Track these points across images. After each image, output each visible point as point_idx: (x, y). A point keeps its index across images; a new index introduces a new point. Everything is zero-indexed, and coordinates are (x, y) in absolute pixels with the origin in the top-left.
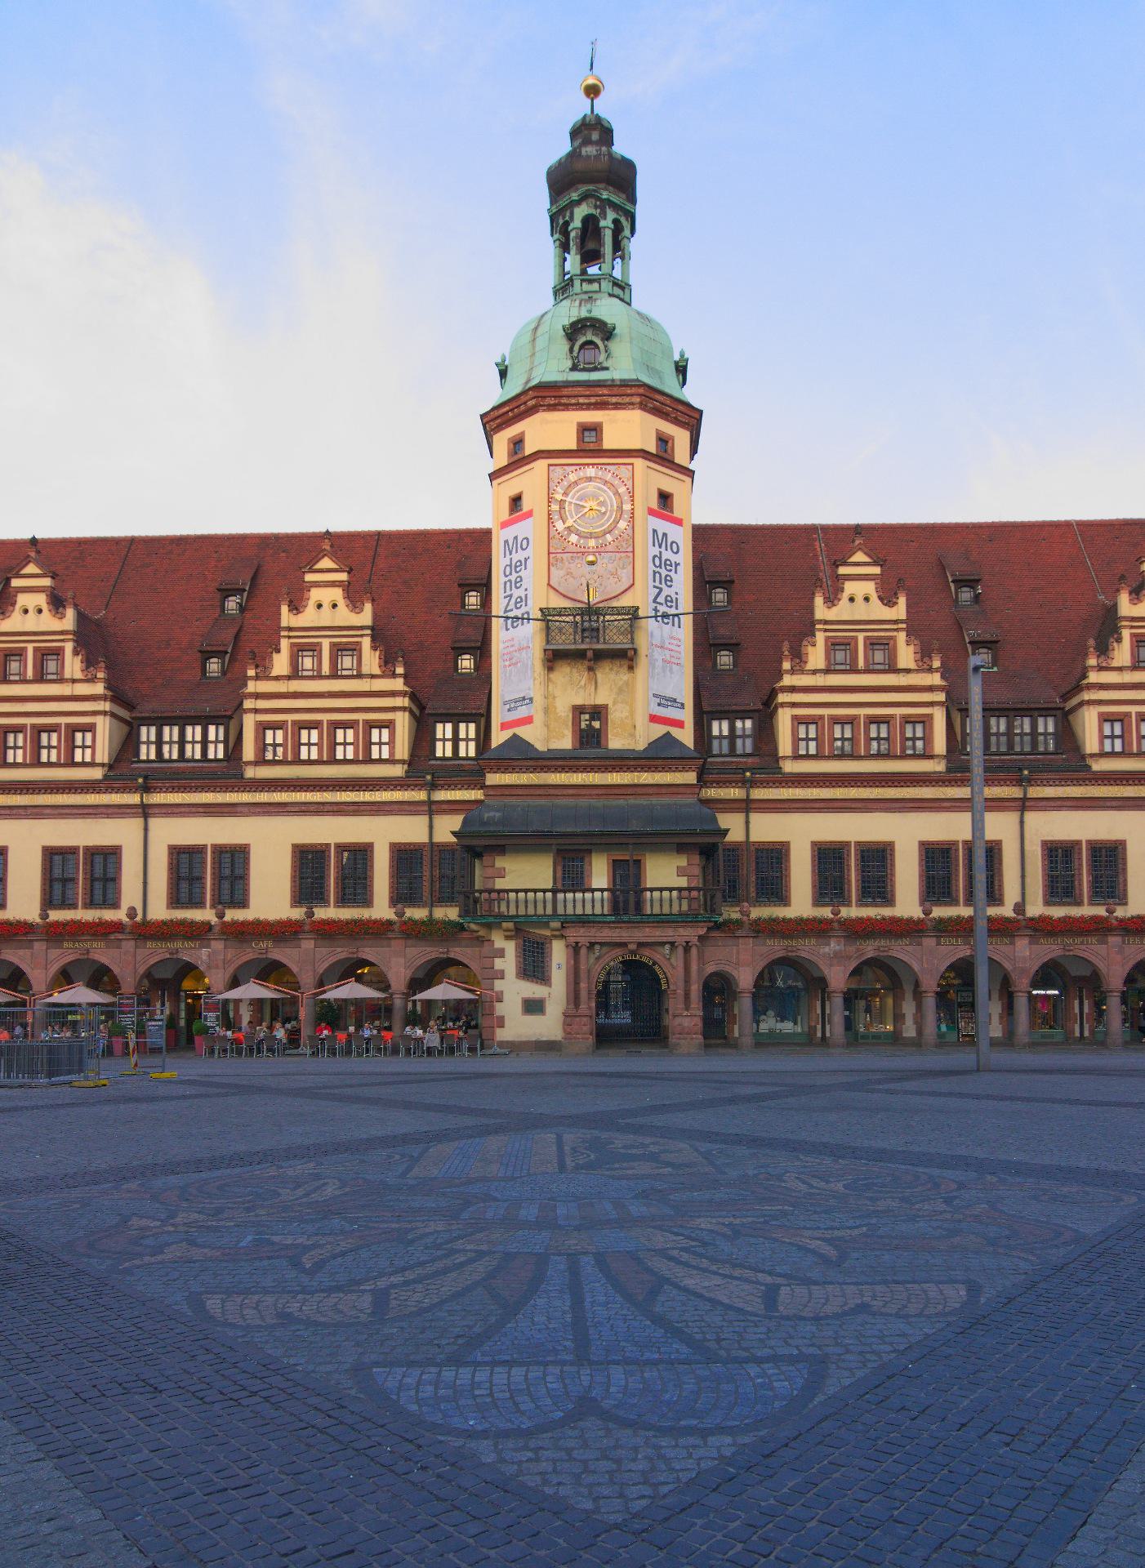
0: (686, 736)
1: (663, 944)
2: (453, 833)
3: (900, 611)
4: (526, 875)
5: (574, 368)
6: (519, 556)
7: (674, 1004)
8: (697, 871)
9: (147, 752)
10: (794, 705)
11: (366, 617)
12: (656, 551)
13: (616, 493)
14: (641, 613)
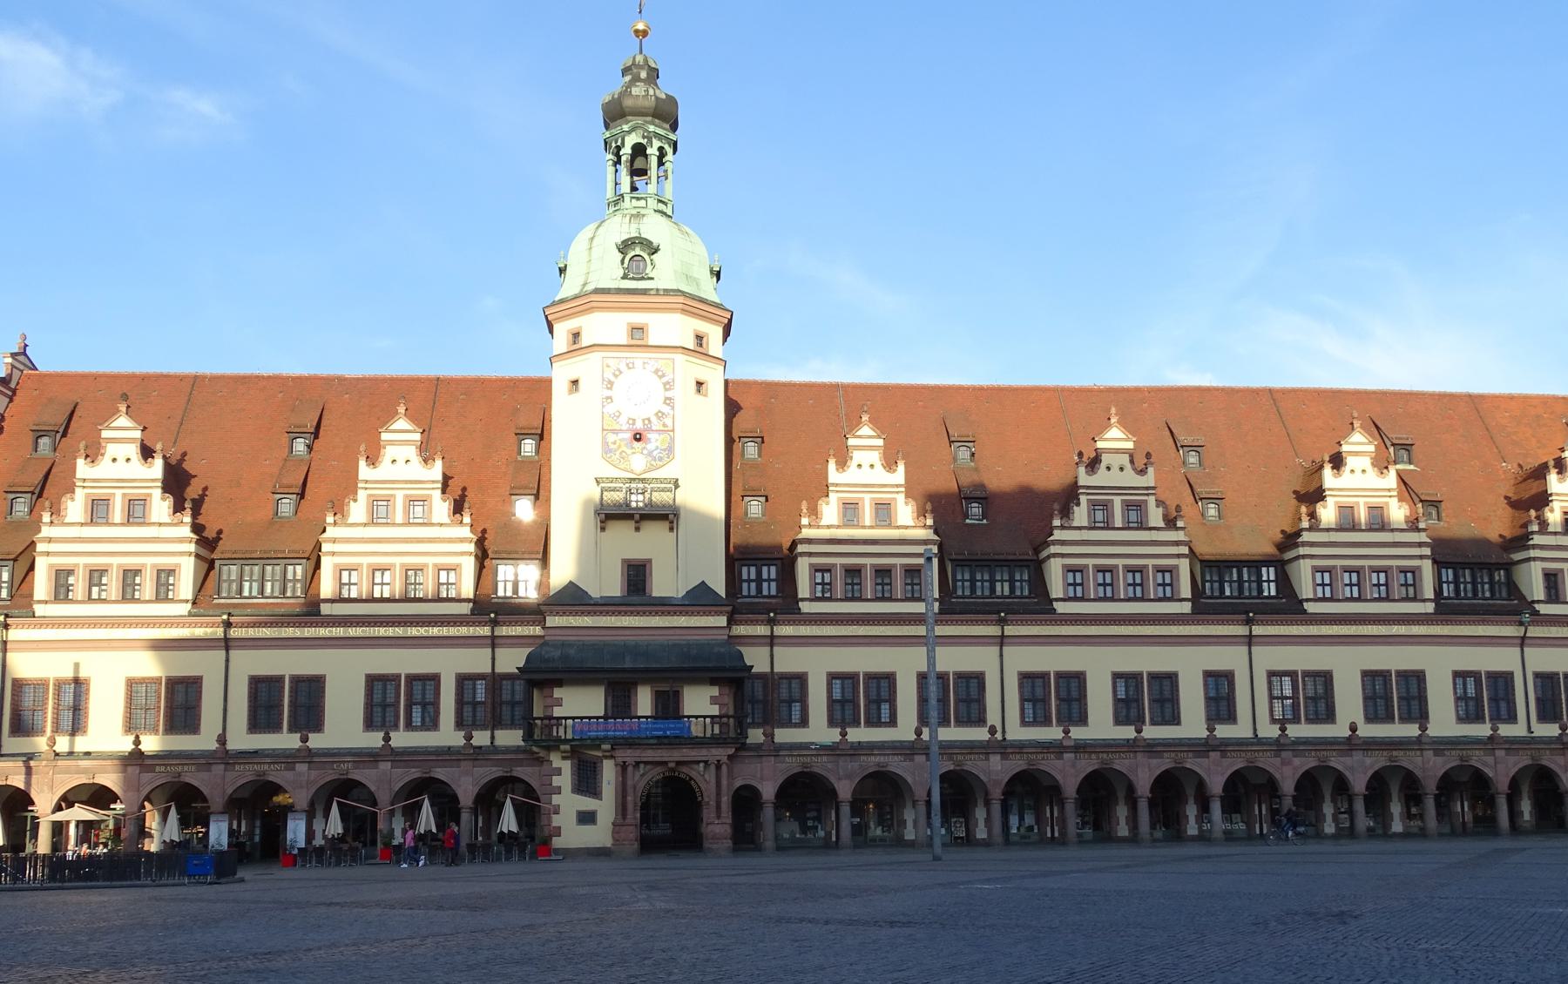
0: (720, 587)
1: (698, 762)
3: (899, 476)
4: (581, 704)
7: (708, 814)
10: (810, 554)
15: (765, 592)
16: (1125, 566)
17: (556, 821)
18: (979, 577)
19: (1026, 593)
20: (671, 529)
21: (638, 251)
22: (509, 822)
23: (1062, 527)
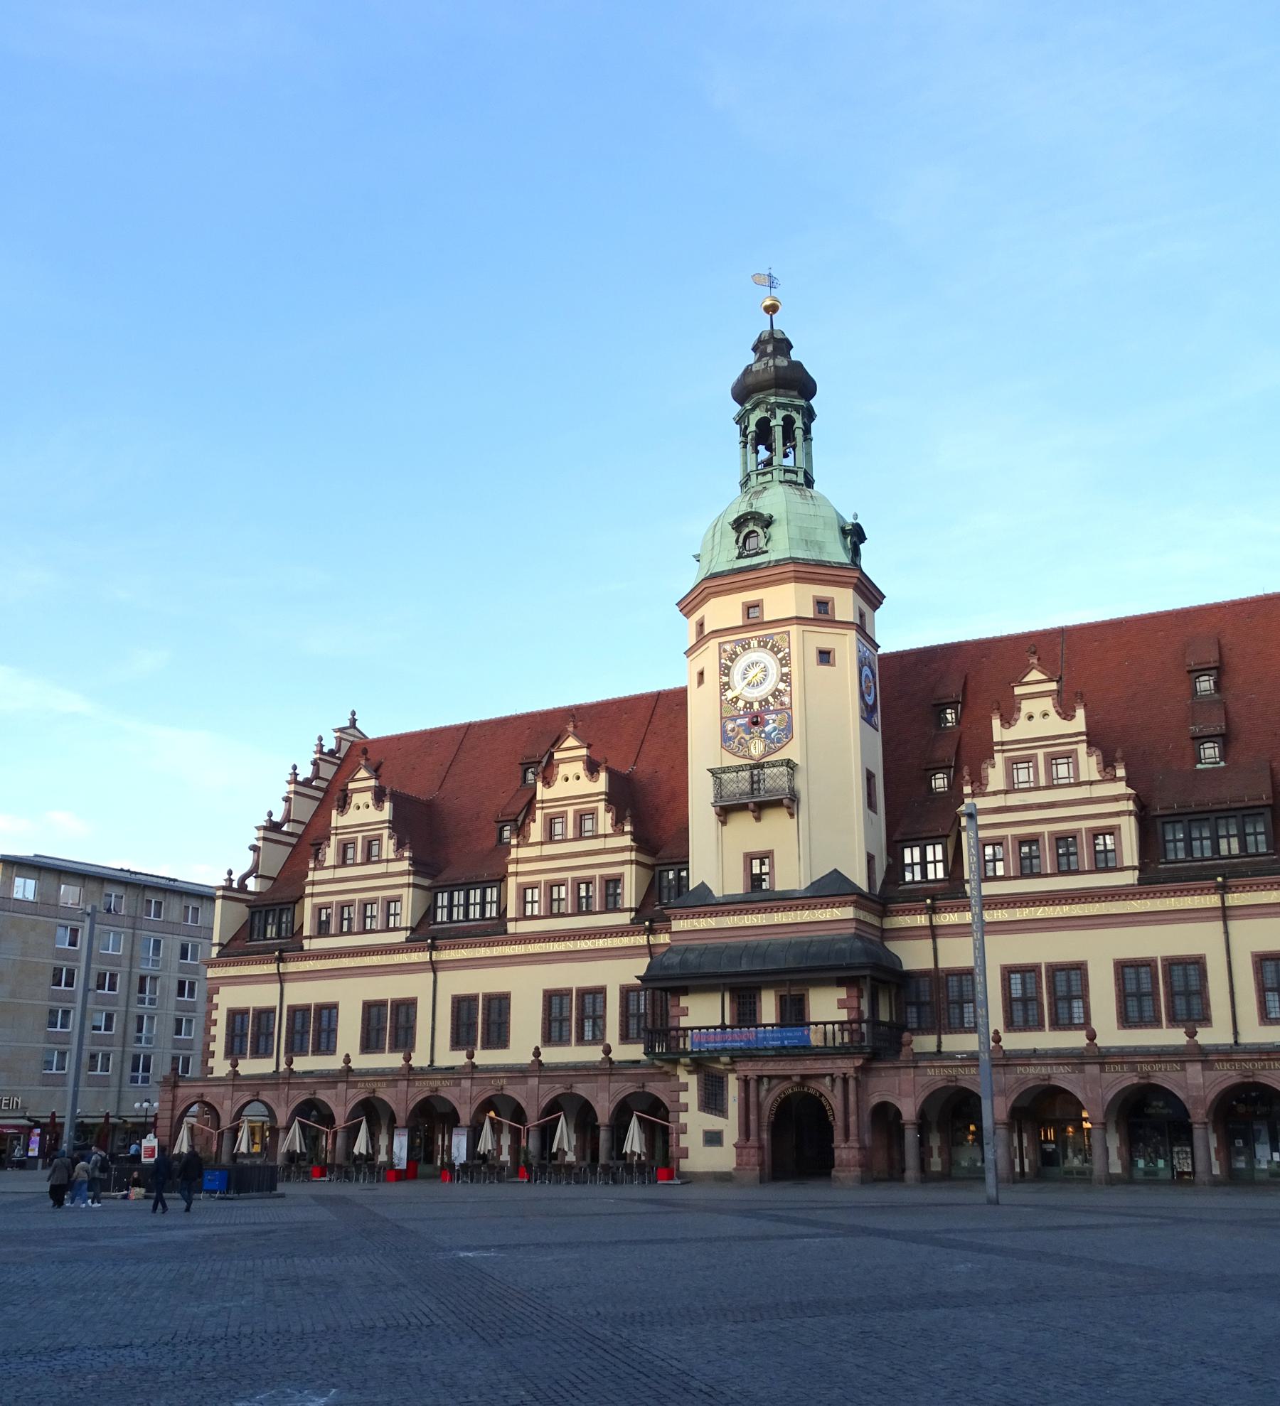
1: (824, 1076)
2: (638, 977)
4: (703, 1012)
5: (740, 556)
9: (442, 915)
17: (684, 1141)
18: (1195, 834)
19: (1263, 849)
20: (792, 815)
21: (751, 527)
22: (634, 1142)
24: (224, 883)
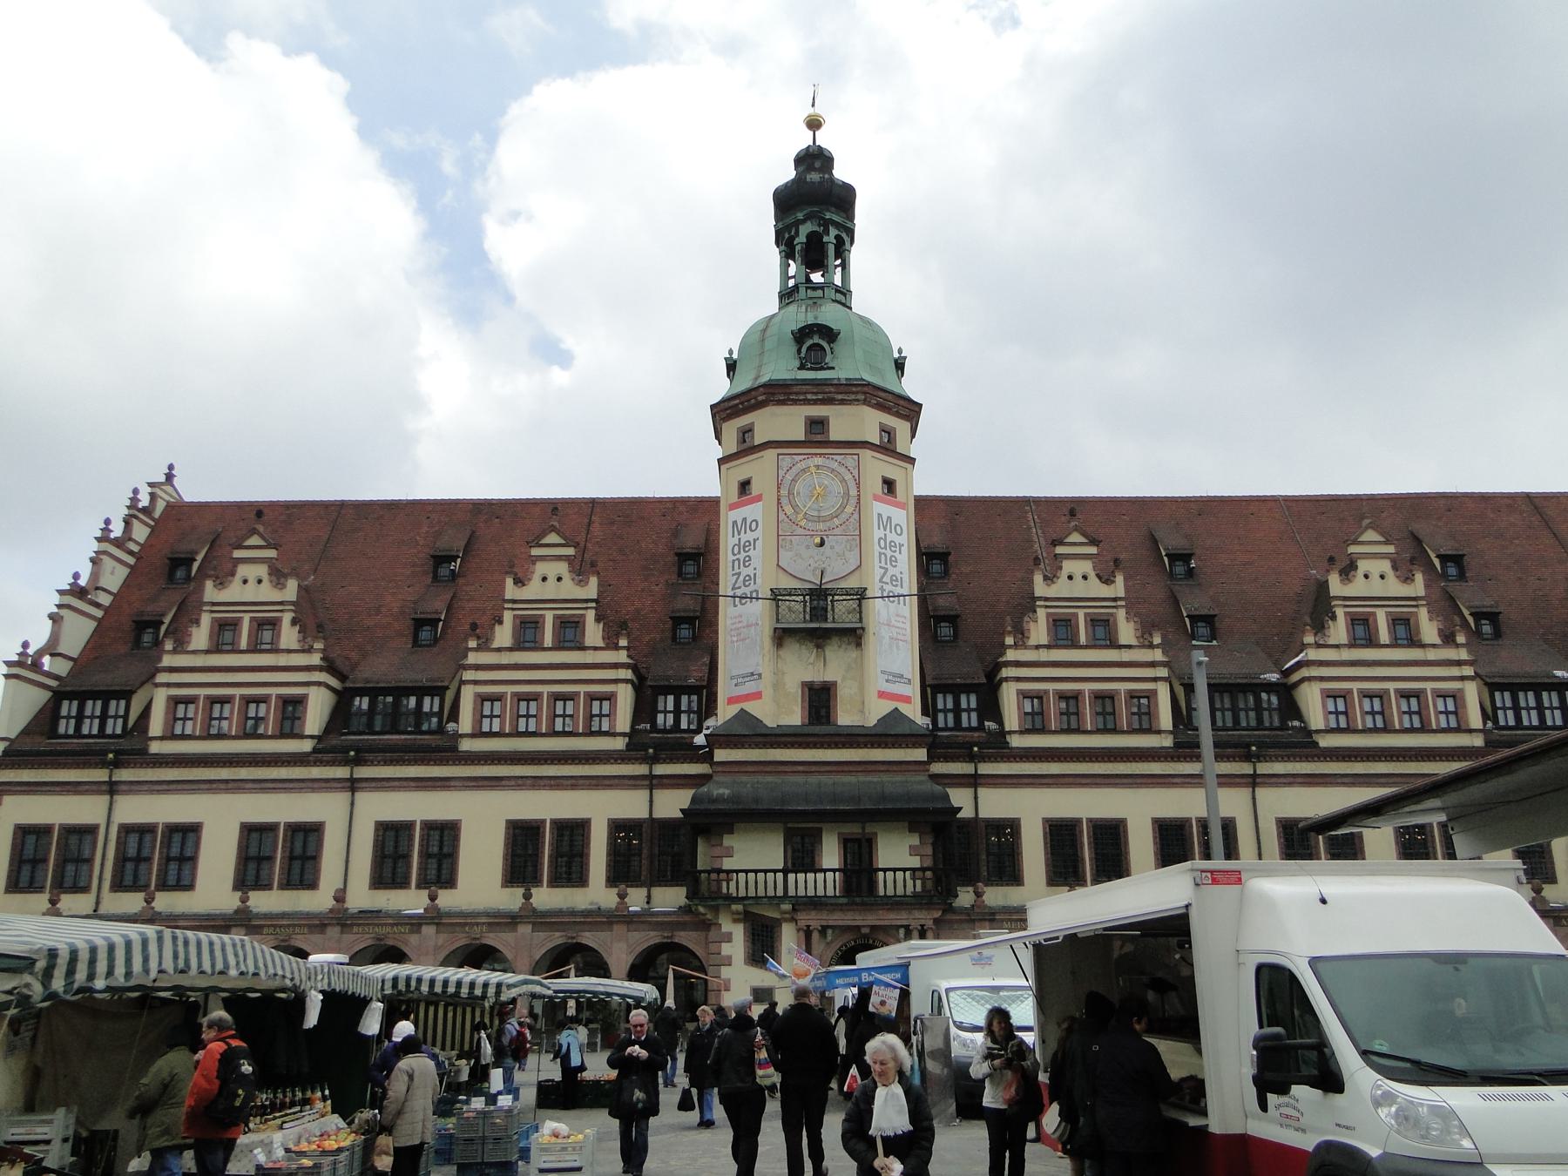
3: (1119, 588)
4: (753, 856)
5: (802, 367)
6: (750, 536)
8: (929, 850)
11: (591, 589)
12: (881, 533)
13: (843, 481)
14: (869, 594)
15: (965, 724)
16: (1396, 691)
21: (816, 340)
23: (1318, 646)
24: (16, 658)
